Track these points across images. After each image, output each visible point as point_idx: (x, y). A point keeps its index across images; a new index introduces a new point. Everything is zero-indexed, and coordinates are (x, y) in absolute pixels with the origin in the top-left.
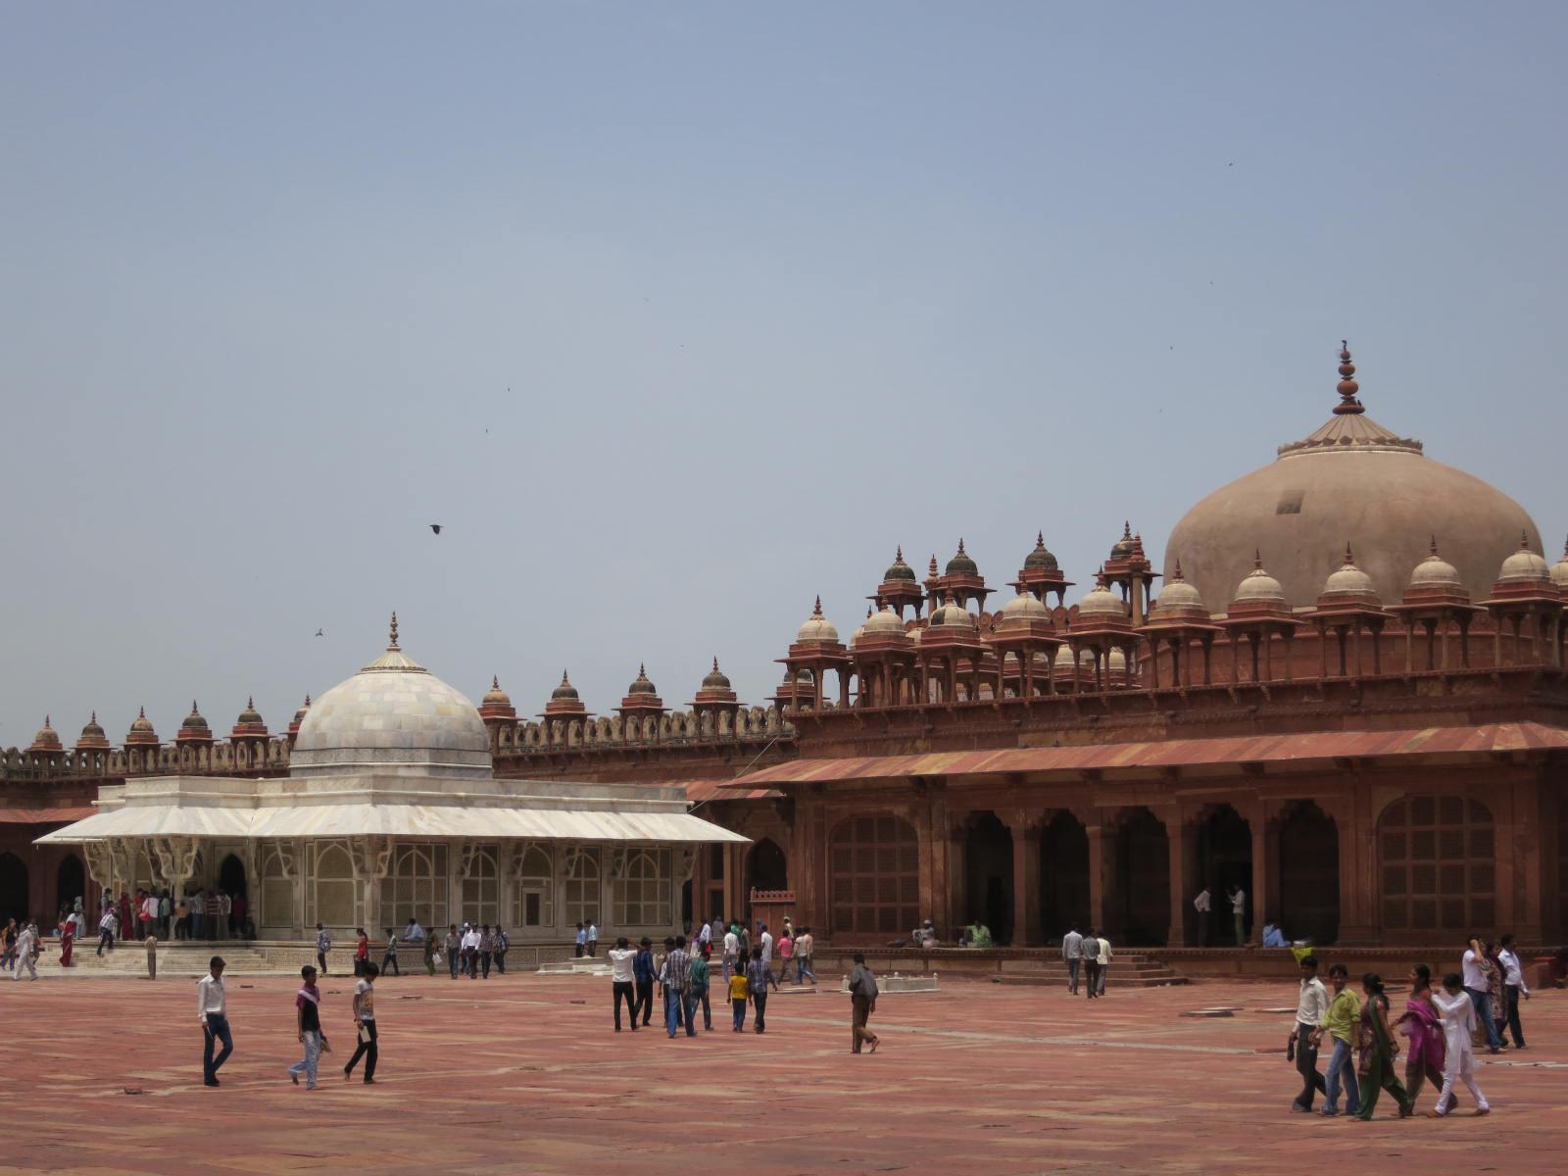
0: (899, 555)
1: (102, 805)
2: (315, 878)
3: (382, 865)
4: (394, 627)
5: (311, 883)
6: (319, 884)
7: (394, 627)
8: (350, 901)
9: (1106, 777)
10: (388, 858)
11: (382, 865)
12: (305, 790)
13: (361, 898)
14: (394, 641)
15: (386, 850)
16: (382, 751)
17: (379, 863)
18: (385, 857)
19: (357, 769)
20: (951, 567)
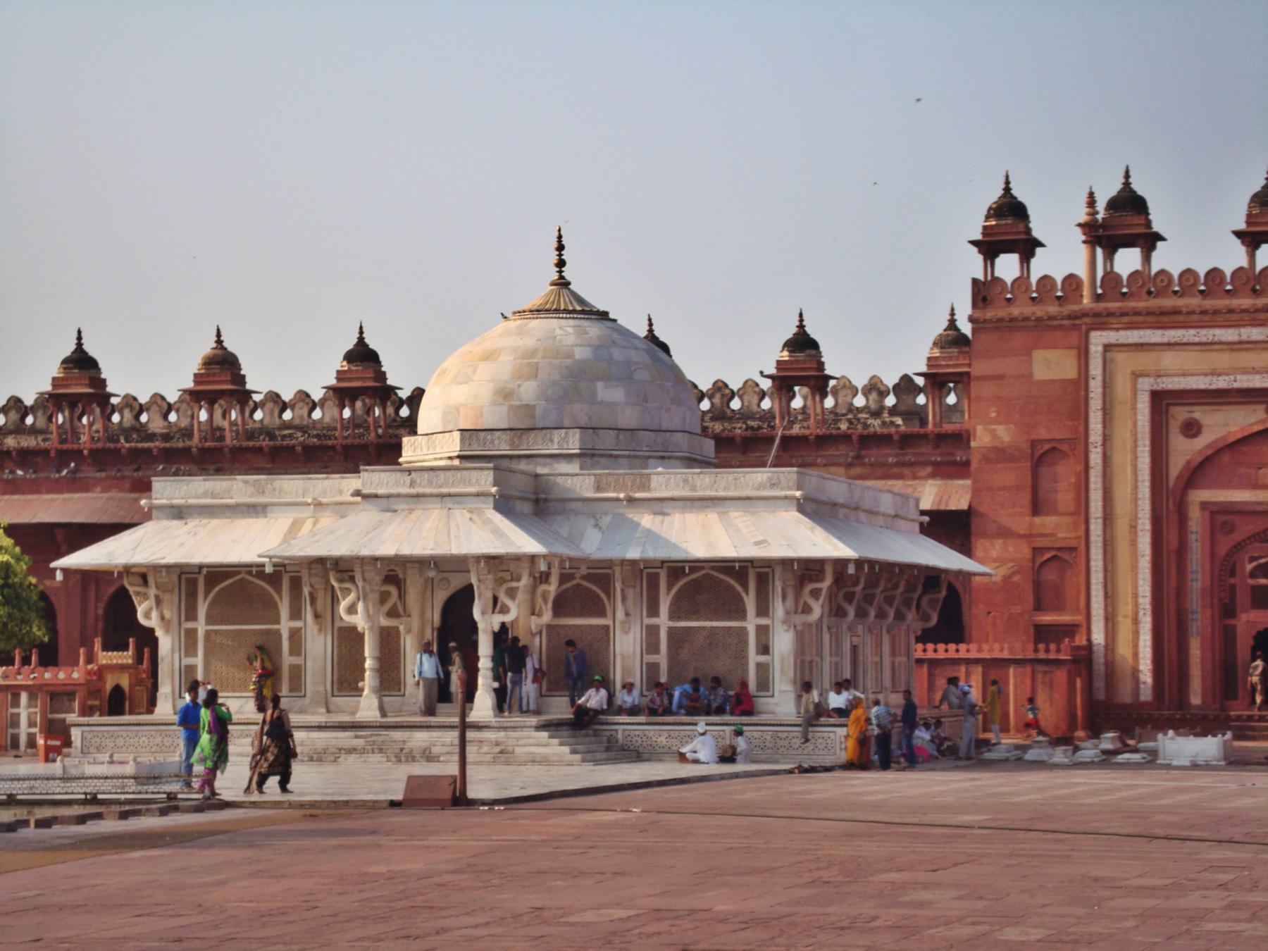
0: (1007, 182)
1: (161, 508)
2: (663, 621)
3: (811, 602)
4: (560, 248)
5: (652, 631)
6: (672, 632)
7: (560, 248)
8: (741, 655)
10: (824, 593)
11: (811, 602)
12: (649, 489)
13: (764, 649)
14: (560, 272)
15: (822, 580)
16: (628, 433)
17: (841, 601)
18: (820, 590)
19: (596, 459)
20: (1113, 204)
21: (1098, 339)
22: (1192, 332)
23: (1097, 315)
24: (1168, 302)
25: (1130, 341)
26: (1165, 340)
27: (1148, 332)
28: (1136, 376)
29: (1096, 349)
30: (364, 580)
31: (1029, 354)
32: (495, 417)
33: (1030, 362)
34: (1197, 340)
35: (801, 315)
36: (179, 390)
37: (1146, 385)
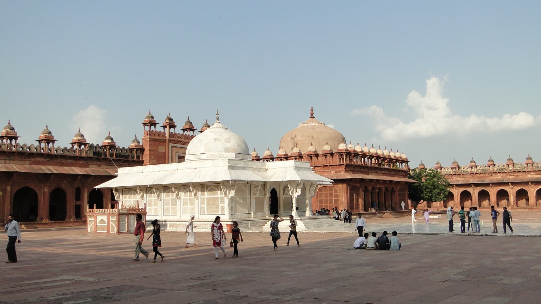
7: (218, 114)
9: (401, 183)
21: (171, 145)
22: (183, 145)
23: (171, 140)
24: (180, 139)
25: (175, 146)
26: (180, 146)
27: (177, 144)
28: (176, 152)
29: (170, 147)
30: (290, 186)
31: (158, 146)
32: (239, 151)
33: (158, 148)
34: (184, 147)
35: (109, 132)
36: (196, 136)
37: (177, 154)
